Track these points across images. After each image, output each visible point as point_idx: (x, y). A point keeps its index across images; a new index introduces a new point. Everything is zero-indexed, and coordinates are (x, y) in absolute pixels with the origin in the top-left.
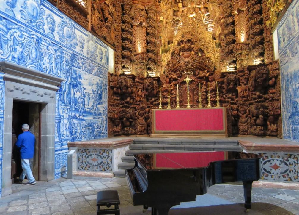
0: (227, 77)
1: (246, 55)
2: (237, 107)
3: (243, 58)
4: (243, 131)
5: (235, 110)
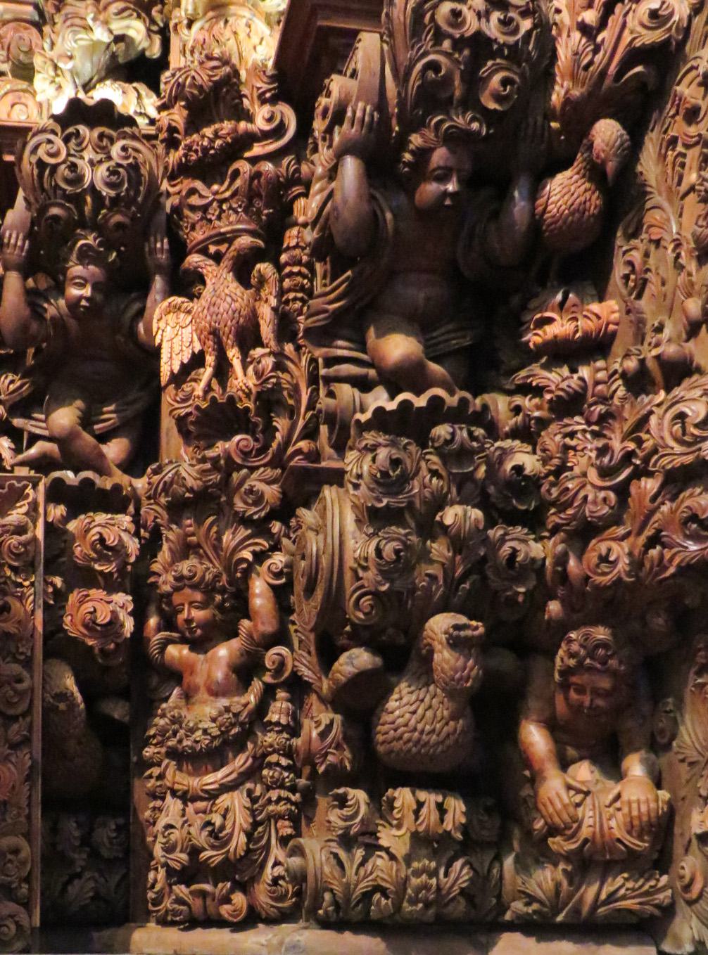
2: (133, 546)
4: (186, 875)
5: (111, 585)
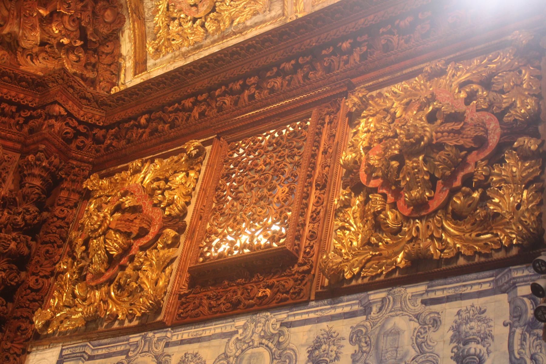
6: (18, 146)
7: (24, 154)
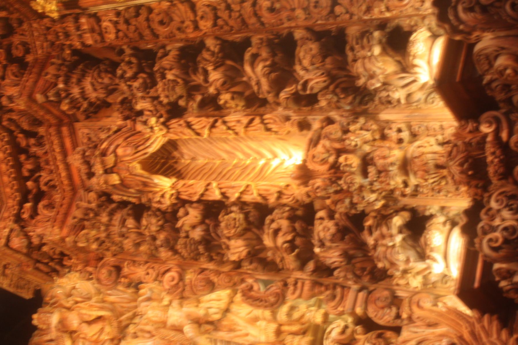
0: (495, 249)
1: (384, 137)
3: (397, 154)
6: (65, 130)
7: (73, 120)
